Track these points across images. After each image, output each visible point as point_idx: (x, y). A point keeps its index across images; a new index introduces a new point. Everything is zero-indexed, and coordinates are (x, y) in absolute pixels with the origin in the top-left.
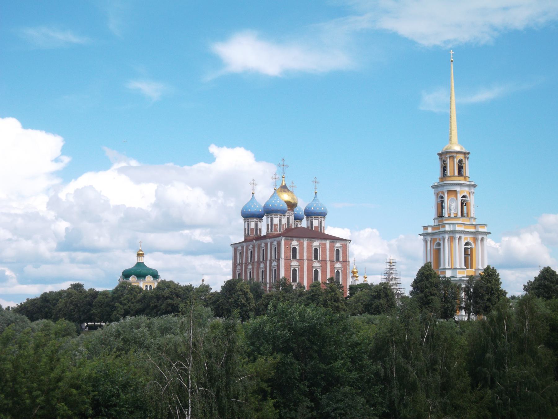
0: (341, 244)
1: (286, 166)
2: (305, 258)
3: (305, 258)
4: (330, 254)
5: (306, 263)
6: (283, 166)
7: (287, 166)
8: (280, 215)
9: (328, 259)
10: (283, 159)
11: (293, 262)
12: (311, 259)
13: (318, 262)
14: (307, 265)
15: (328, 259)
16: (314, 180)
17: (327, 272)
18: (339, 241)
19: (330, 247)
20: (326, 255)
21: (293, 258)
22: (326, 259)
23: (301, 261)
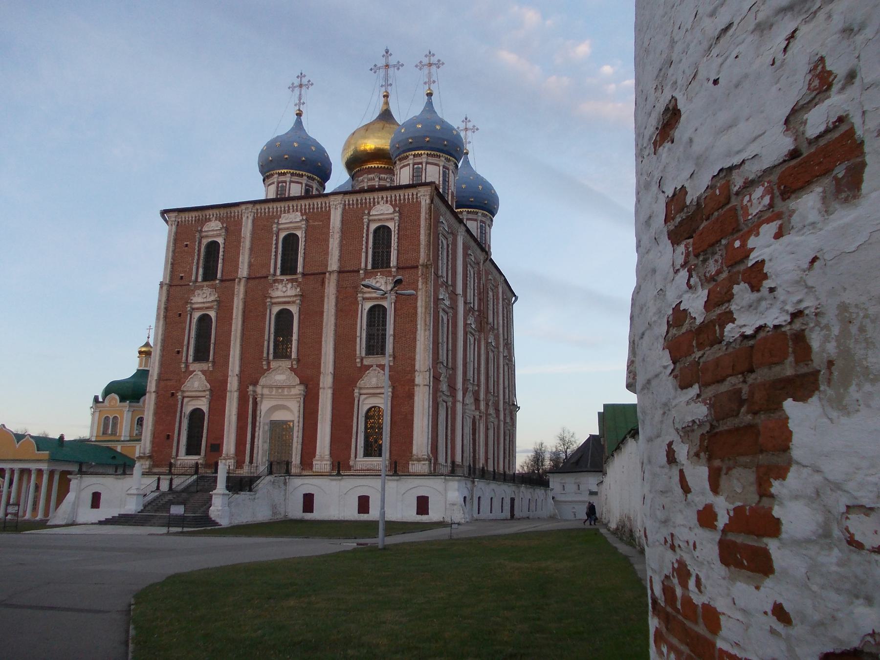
0: (394, 206)
1: (394, 66)
2: (243, 271)
3: (243, 271)
4: (342, 246)
5: (240, 290)
6: (387, 66)
7: (399, 66)
8: (280, 174)
9: (333, 264)
10: (387, 52)
11: (196, 293)
12: (263, 273)
13: (292, 281)
14: (246, 292)
15: (333, 264)
16: (426, 61)
17: (322, 312)
18: (384, 194)
19: (343, 222)
20: (326, 252)
21: (205, 279)
22: (327, 266)
23: (227, 284)
